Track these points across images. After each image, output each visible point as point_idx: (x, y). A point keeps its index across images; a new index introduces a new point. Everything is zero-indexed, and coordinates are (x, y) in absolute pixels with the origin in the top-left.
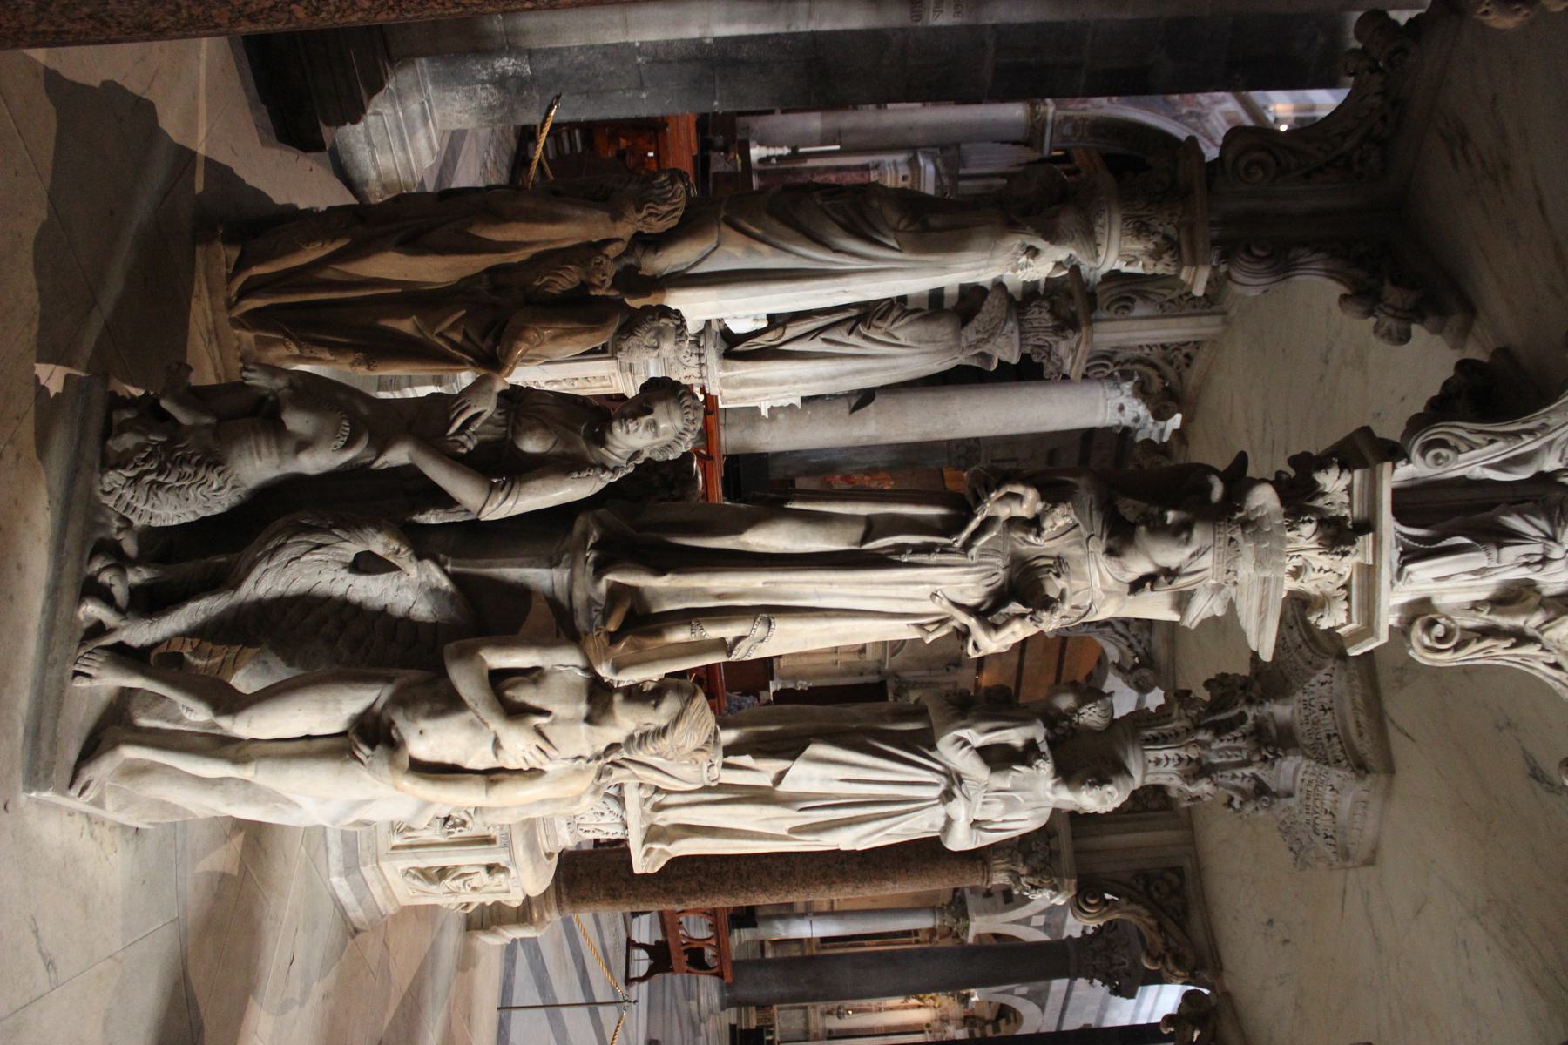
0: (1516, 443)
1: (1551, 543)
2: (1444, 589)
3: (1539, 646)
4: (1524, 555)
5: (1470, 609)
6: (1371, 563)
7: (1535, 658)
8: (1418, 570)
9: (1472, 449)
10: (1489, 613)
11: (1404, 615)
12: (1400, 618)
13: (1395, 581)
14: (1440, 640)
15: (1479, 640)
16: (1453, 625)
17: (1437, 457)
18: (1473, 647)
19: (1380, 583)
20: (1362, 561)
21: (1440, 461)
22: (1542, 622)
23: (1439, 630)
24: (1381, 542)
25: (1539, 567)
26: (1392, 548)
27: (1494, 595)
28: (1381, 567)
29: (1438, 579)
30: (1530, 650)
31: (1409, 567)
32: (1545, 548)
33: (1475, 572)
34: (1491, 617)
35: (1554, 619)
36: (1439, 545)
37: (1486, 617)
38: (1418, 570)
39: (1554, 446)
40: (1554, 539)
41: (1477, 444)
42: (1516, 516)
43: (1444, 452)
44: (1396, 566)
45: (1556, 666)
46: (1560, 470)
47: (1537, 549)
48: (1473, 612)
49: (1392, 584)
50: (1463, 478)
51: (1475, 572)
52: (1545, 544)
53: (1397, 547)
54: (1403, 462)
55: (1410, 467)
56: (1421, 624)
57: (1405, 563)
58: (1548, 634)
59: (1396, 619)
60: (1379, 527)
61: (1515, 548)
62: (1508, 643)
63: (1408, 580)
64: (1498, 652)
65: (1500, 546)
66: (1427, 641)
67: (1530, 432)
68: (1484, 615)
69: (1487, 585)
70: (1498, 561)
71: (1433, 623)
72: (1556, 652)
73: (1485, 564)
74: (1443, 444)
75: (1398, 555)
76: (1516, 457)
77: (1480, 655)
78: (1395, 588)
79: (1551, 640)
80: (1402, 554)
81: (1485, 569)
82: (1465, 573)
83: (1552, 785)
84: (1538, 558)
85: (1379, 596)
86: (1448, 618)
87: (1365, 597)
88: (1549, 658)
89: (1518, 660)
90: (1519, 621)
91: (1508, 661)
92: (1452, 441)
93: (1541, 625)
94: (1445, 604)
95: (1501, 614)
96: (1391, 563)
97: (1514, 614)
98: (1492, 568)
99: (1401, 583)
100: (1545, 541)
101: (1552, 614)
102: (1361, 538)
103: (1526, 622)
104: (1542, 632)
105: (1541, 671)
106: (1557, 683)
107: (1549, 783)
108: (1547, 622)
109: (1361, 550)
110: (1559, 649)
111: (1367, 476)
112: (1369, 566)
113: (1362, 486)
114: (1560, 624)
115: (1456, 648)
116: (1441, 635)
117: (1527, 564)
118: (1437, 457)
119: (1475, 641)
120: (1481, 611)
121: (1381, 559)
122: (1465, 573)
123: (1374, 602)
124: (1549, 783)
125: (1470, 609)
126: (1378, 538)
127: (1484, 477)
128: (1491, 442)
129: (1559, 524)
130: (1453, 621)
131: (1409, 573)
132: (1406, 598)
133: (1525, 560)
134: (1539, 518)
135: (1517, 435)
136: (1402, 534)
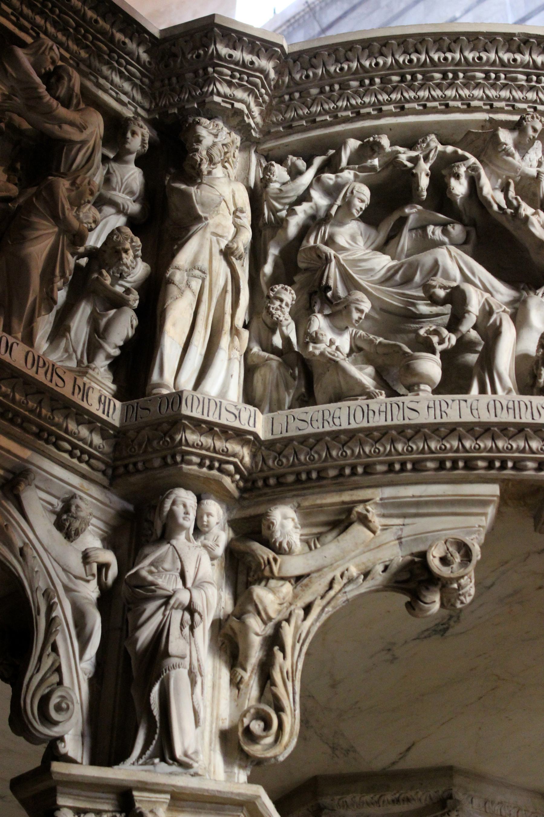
0: (60, 624)
1: (172, 602)
2: (212, 715)
3: (284, 624)
4: (181, 630)
5: (239, 689)
6: (169, 796)
7: (297, 628)
8: (183, 743)
9: (58, 670)
10: (245, 669)
11: (238, 762)
12: (242, 767)
13: (192, 771)
14: (267, 726)
15: (274, 684)
16: (252, 711)
17: (58, 708)
18: (280, 691)
19: (193, 789)
20: (165, 806)
21: (64, 705)
22: (258, 619)
23: (257, 727)
24: (146, 783)
25: (197, 616)
26: (155, 772)
27: (226, 662)
28: (173, 786)
29: (197, 723)
30: (288, 632)
31: (179, 753)
32: (177, 608)
33: (193, 683)
34: (249, 668)
35: (256, 606)
36: (157, 718)
37: (249, 674)
38: (183, 743)
39: (71, 585)
40: (169, 597)
41: (53, 664)
42: (138, 634)
43: (54, 700)
44: (175, 768)
45: (307, 609)
46: (99, 583)
47: (176, 616)
48: (242, 686)
49: (195, 775)
50: (91, 682)
51: (193, 683)
52: (173, 607)
53: (153, 764)
54: (61, 746)
55: (67, 738)
56: (247, 744)
57: (173, 758)
58: (272, 614)
59: (241, 771)
60: (125, 784)
61: (171, 638)
62: (279, 655)
63: (193, 756)
64: (288, 665)
65: (166, 654)
66: (269, 740)
67: (50, 608)
68: (246, 676)
69: (214, 668)
70: (183, 657)
71: (247, 731)
72: (292, 607)
73: (184, 673)
74: (45, 700)
75: (163, 764)
76: (76, 626)
77: (289, 684)
78: (200, 772)
79: (279, 612)
80: (163, 760)
81: (191, 673)
82: (192, 694)
83: (451, 617)
84: (187, 616)
85: (207, 791)
86: (244, 715)
87: (208, 805)
88: (299, 615)
89: (298, 646)
90: (256, 642)
91: (299, 656)
92: (44, 690)
93: (262, 619)
94: (230, 715)
95: (246, 658)
96: (171, 774)
97: (248, 645)
98: (191, 664)
99: (195, 765)
100: (169, 607)
101: (251, 608)
102: (137, 805)
103: (257, 634)
104: (270, 619)
105: (312, 624)
106: (326, 609)
107: (449, 619)
108: (259, 614)
109: (151, 806)
110: (291, 604)
111: (66, 790)
112: (172, 798)
113: (77, 797)
114: (262, 602)
115: (279, 709)
116: (262, 724)
117: (192, 628)
118: (58, 708)
119: (273, 688)
120: (242, 678)
121: (164, 785)
122: (192, 694)
123: (214, 797)
124: (449, 619)
125: (239, 689)
126: (139, 785)
127: (94, 660)
128: (55, 649)
129: (154, 591)
130: (248, 711)
131: (186, 755)
132: (218, 759)
133: (187, 630)
134: (144, 610)
135: (51, 622)
136: (140, 757)
